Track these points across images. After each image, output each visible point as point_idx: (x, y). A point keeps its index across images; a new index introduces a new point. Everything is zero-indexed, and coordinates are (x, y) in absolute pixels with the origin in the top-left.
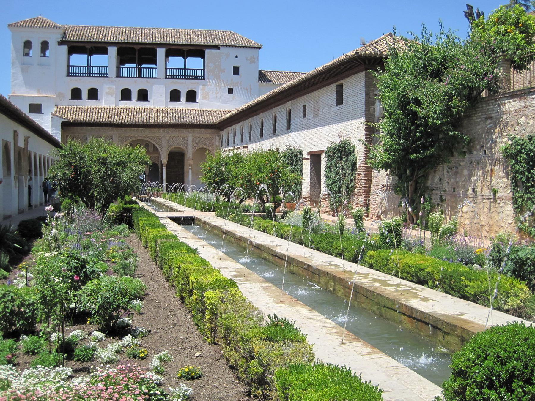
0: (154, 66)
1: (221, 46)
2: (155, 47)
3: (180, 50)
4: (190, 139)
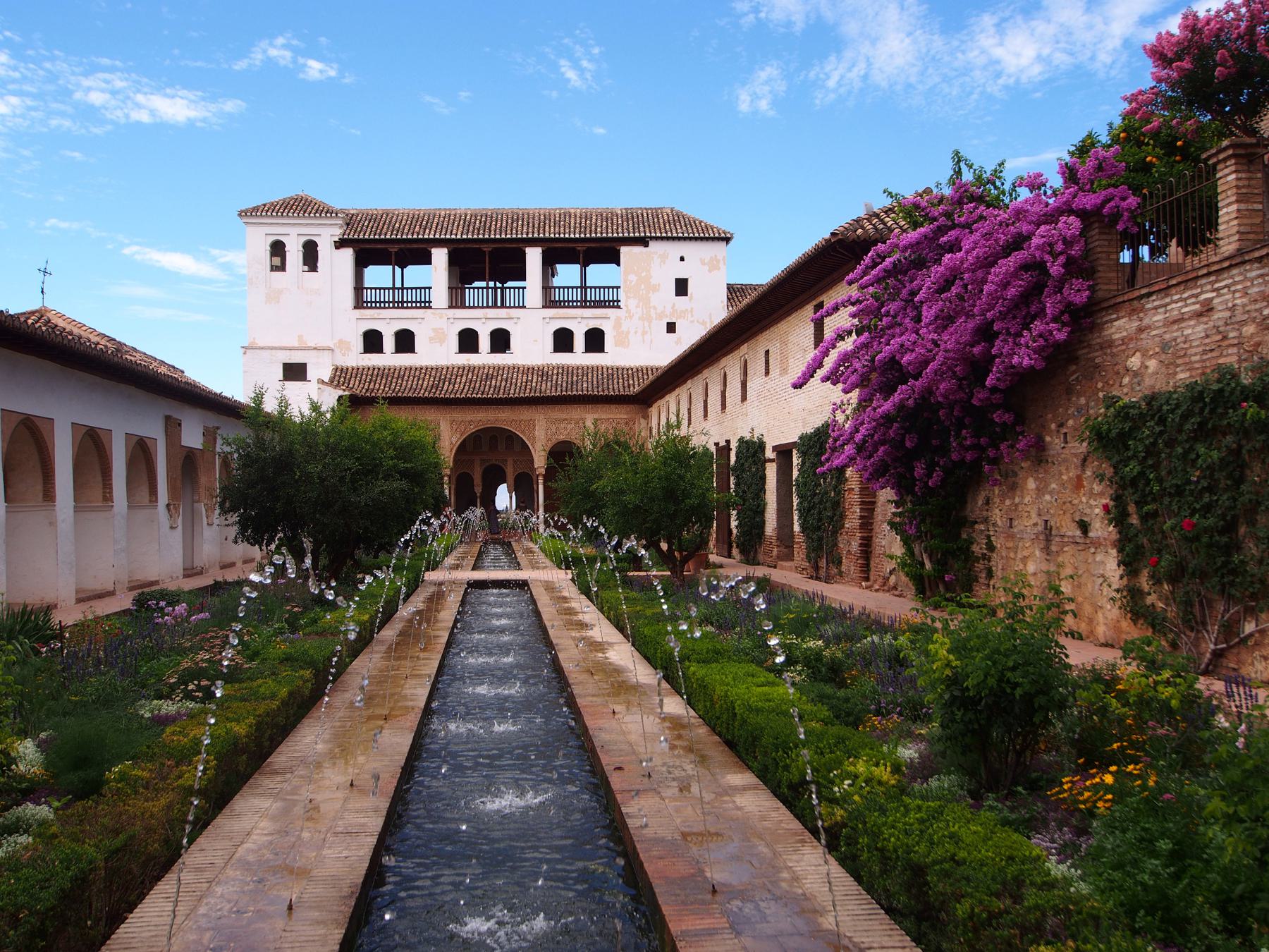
1: (651, 238)
3: (574, 249)
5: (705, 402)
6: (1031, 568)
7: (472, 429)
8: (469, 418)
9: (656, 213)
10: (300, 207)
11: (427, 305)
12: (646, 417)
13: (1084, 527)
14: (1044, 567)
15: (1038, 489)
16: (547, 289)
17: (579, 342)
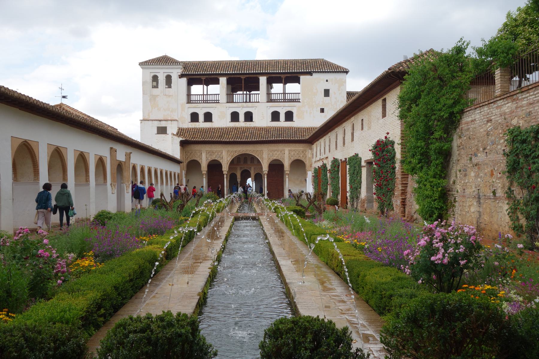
1: (314, 72)
2: (257, 76)
3: (280, 77)
4: (287, 152)
5: (336, 142)
6: (472, 209)
7: (236, 154)
8: (235, 149)
9: (316, 61)
10: (165, 61)
12: (311, 149)
13: (494, 193)
14: (478, 209)
15: (475, 176)
16: (269, 94)
17: (282, 117)
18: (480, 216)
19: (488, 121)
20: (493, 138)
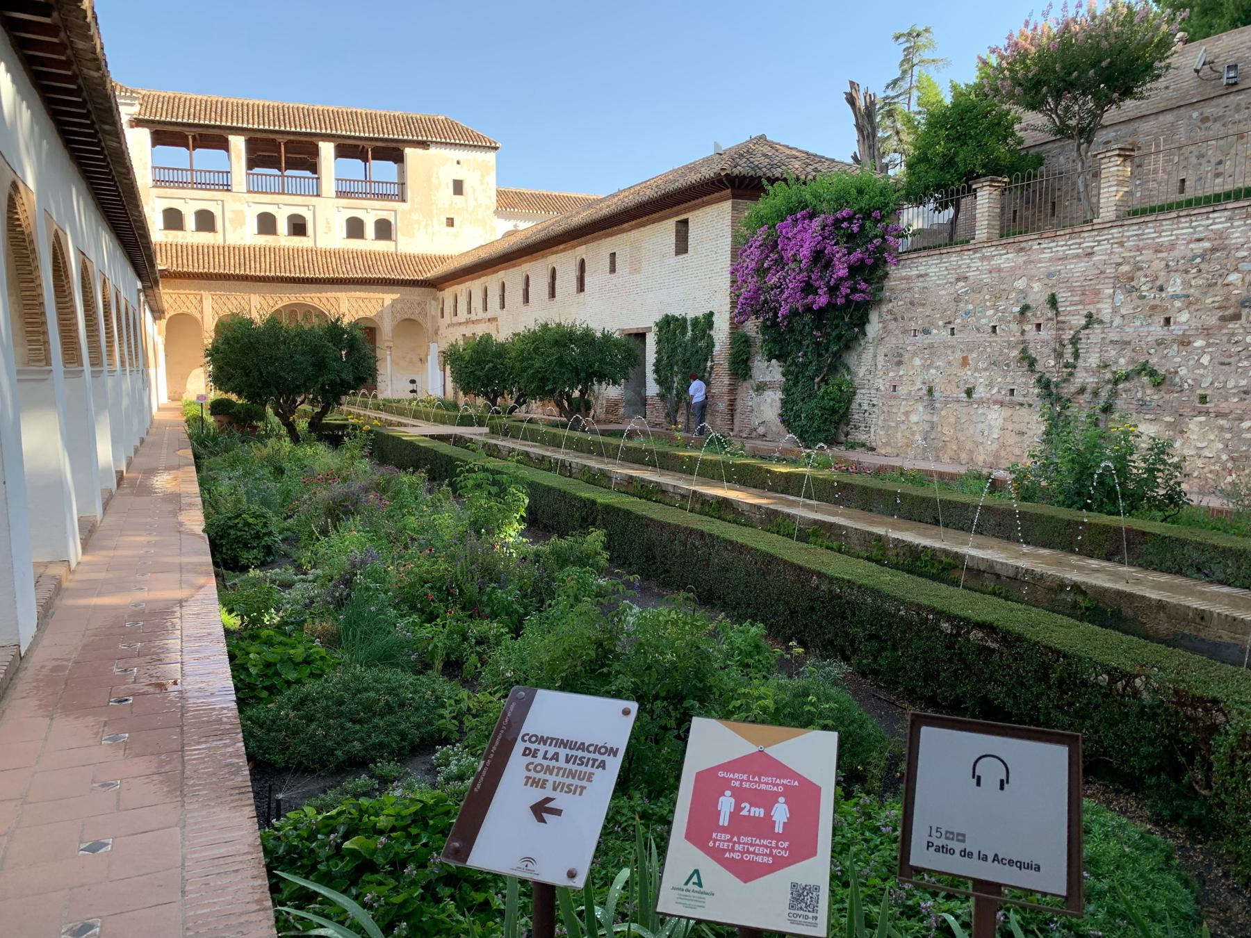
0: (307, 173)
2: (314, 139)
11: (227, 188)
13: (969, 392)
18: (932, 428)
19: (958, 280)
20: (970, 307)
